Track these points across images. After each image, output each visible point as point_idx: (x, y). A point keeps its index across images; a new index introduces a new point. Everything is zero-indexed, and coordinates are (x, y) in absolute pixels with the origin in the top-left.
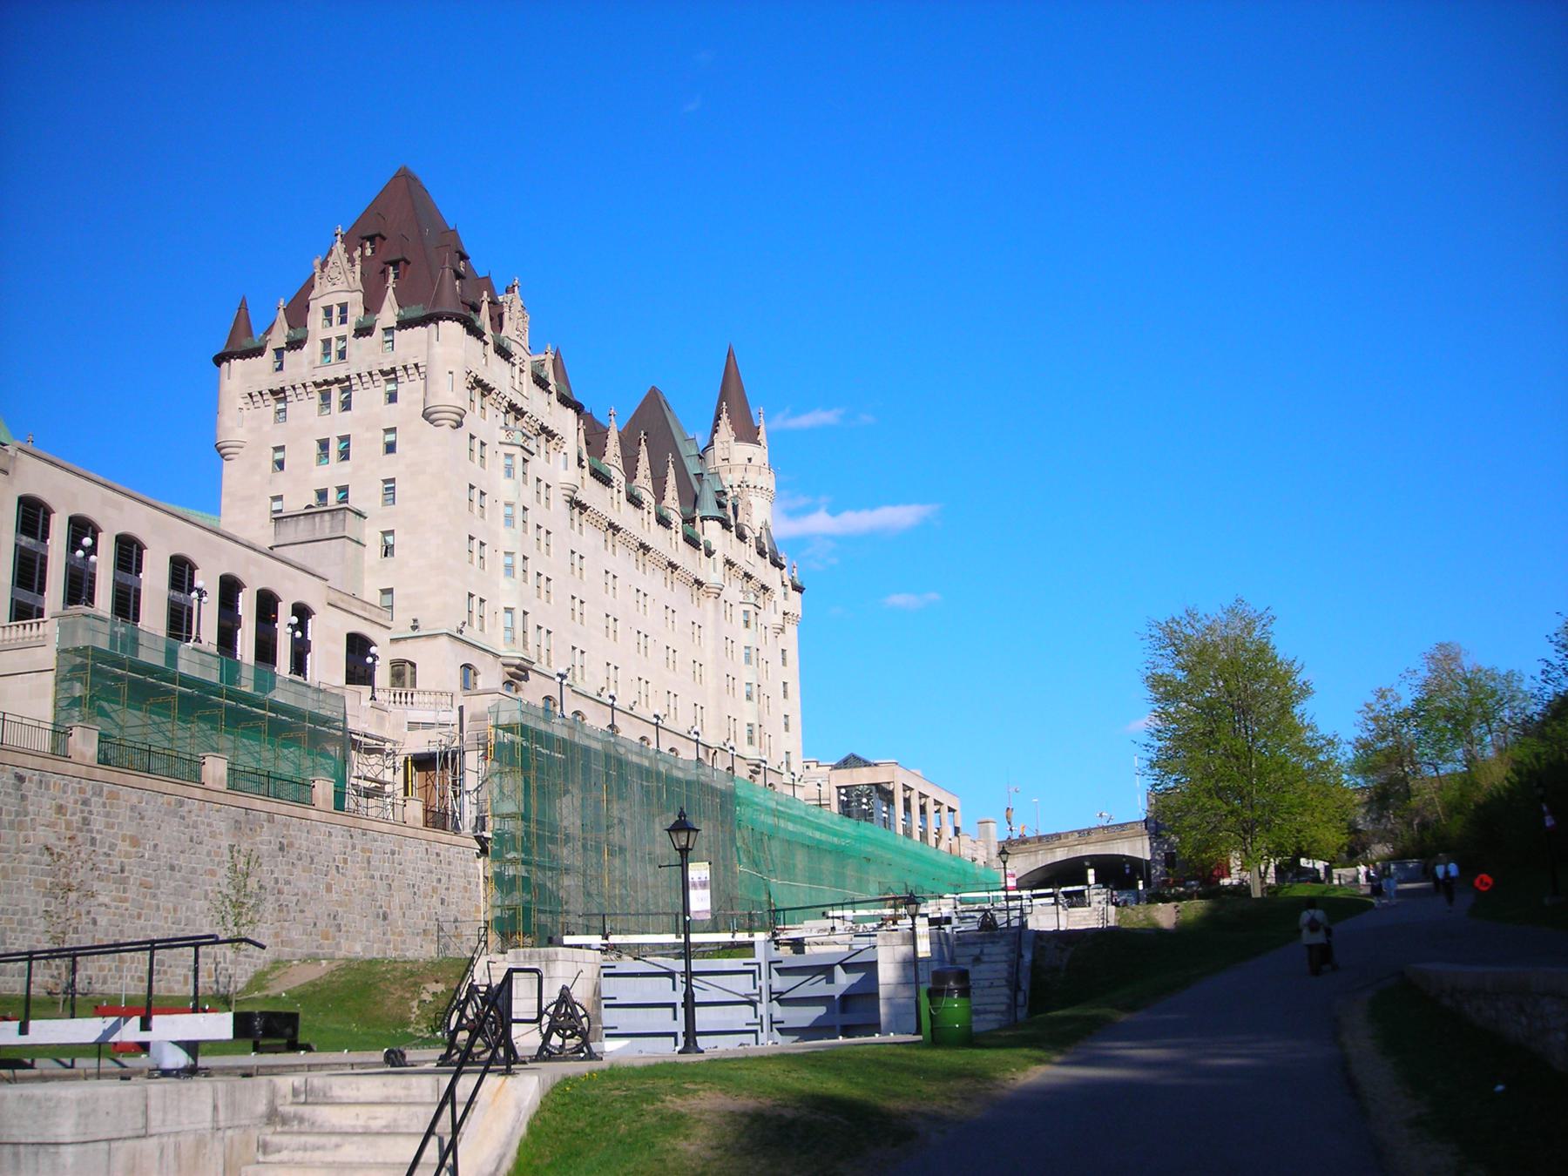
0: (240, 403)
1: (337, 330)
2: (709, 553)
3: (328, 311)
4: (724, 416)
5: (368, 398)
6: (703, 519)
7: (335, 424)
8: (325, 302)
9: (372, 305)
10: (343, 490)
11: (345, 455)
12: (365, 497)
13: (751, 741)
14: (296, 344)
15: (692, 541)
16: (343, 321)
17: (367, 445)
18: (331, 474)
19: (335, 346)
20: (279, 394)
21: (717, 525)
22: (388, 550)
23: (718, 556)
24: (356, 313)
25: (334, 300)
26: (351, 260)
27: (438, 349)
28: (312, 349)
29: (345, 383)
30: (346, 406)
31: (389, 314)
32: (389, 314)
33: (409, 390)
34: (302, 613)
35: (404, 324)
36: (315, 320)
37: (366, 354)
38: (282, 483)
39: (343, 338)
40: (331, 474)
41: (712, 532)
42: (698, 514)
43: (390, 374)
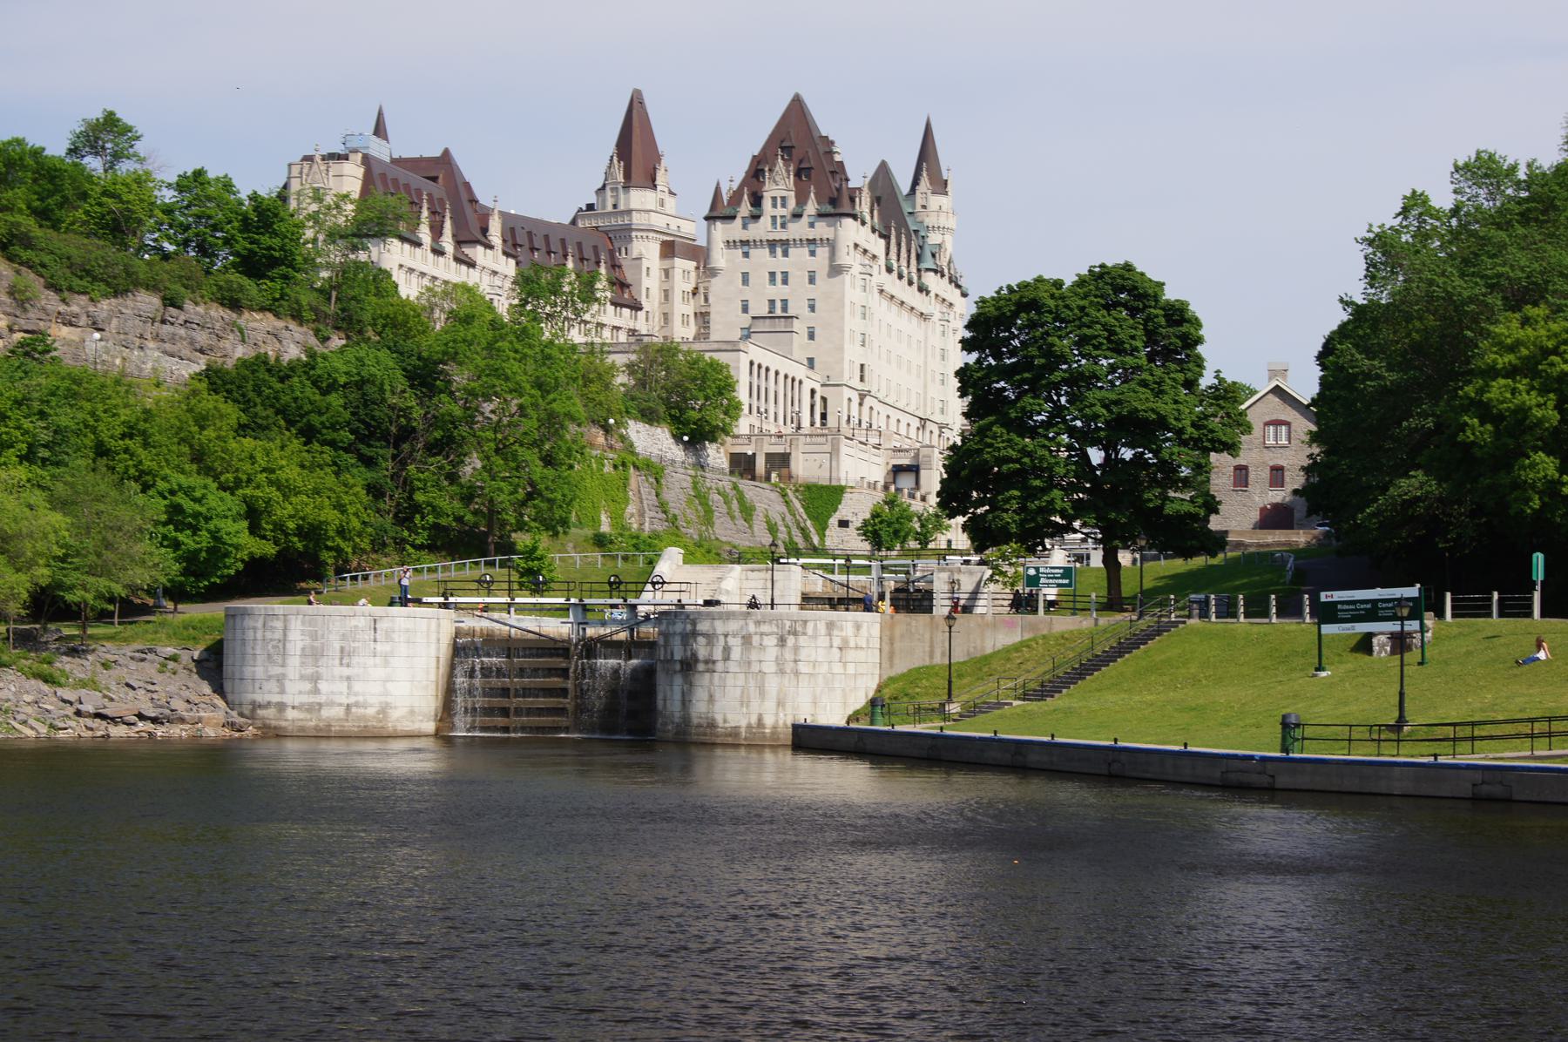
0: (722, 245)
1: (780, 211)
2: (928, 293)
3: (774, 199)
4: (925, 174)
5: (799, 254)
6: (928, 270)
7: (779, 263)
8: (774, 194)
9: (801, 200)
10: (785, 302)
11: (785, 282)
12: (798, 307)
13: (942, 412)
14: (756, 217)
15: (922, 289)
16: (784, 206)
17: (798, 277)
18: (778, 291)
19: (779, 221)
20: (745, 243)
21: (932, 274)
22: (811, 336)
23: (932, 295)
24: (792, 203)
25: (778, 194)
26: (788, 172)
27: (841, 232)
28: (765, 221)
29: (785, 243)
30: (785, 254)
31: (811, 208)
32: (811, 208)
33: (823, 252)
34: (800, 382)
35: (821, 215)
36: (767, 203)
37: (798, 230)
38: (747, 293)
39: (782, 217)
40: (778, 291)
41: (930, 280)
42: (923, 266)
43: (812, 242)
